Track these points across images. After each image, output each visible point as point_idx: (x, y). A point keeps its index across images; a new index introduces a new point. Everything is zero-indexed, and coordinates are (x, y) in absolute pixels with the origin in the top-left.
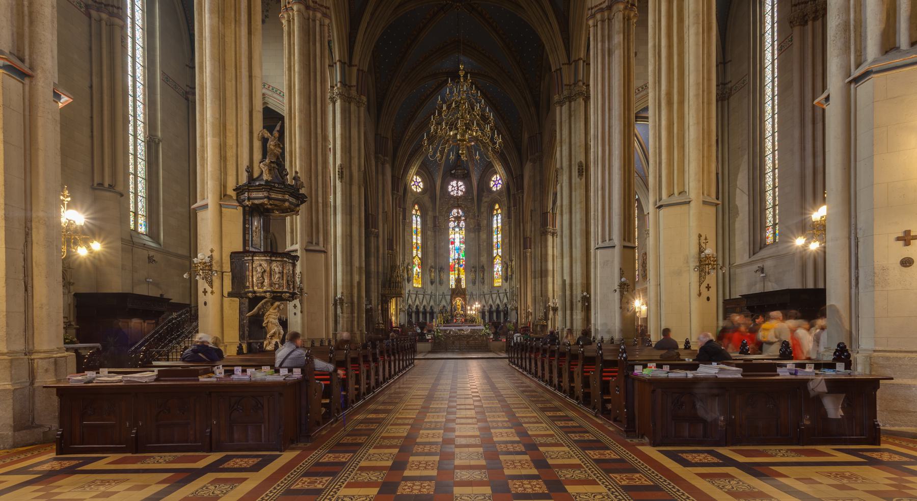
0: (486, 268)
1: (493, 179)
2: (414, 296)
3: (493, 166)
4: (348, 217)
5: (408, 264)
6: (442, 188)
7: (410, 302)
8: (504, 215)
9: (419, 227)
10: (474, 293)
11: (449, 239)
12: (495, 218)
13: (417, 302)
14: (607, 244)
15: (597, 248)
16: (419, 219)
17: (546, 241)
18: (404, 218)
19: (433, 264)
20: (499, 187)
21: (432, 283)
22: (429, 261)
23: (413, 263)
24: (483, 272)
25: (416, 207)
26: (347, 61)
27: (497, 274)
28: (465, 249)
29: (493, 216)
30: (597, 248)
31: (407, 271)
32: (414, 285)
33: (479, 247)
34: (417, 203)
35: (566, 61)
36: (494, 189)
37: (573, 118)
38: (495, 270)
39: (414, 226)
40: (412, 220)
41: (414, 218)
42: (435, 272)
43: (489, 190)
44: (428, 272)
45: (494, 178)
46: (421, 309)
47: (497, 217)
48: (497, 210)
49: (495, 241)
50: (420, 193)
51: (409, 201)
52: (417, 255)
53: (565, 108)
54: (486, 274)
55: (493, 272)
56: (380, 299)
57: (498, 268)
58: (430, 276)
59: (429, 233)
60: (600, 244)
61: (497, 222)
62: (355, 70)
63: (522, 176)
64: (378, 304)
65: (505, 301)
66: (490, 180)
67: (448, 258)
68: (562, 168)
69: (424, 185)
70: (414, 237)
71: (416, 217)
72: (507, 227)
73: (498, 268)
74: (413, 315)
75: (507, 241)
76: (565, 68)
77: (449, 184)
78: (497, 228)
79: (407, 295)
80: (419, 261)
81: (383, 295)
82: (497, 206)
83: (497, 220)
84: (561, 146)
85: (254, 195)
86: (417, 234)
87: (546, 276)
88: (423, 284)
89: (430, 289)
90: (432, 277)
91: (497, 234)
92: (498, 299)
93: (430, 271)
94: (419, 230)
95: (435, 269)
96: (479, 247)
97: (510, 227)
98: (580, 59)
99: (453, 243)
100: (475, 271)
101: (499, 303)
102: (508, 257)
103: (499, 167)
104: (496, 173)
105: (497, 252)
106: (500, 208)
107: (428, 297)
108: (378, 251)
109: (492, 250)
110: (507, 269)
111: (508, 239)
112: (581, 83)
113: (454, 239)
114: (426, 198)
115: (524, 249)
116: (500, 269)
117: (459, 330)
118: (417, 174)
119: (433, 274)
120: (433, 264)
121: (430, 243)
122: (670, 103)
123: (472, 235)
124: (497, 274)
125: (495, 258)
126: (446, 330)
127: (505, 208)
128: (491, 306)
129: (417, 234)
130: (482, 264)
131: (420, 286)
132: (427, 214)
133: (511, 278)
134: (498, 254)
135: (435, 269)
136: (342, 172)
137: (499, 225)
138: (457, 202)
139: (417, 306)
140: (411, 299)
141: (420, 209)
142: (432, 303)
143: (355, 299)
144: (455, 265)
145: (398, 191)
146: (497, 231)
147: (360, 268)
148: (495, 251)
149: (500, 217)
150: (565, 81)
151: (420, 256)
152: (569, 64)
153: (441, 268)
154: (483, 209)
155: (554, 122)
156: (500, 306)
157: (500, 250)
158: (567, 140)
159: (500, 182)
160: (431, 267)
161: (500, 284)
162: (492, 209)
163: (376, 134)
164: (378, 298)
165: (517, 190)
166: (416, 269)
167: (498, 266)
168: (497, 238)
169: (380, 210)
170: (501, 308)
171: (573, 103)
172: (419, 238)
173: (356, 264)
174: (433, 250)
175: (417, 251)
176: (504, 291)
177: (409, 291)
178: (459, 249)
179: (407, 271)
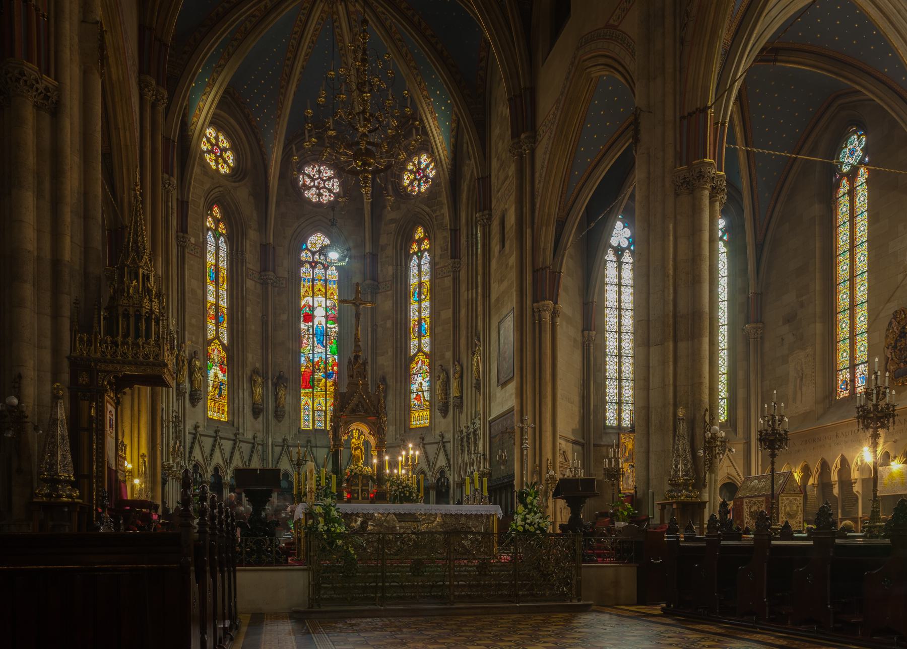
2: (208, 442)
8: (438, 252)
12: (415, 261)
13: (217, 459)
27: (418, 398)
28: (339, 334)
29: (408, 257)
32: (210, 414)
42: (264, 384)
44: (246, 385)
47: (420, 258)
49: (414, 316)
57: (421, 383)
58: (252, 394)
65: (442, 462)
67: (298, 354)
72: (448, 282)
73: (421, 383)
78: (420, 284)
79: (189, 438)
83: (419, 266)
88: (231, 412)
89: (250, 427)
93: (252, 382)
97: (456, 281)
99: (309, 318)
106: (427, 237)
109: (407, 340)
110: (446, 384)
113: (312, 308)
115: (533, 302)
116: (425, 386)
117: (401, 517)
119: (259, 390)
120: (257, 365)
124: (418, 398)
131: (224, 418)
133: (459, 406)
139: (216, 469)
140: (201, 448)
144: (313, 372)
146: (420, 294)
148: (414, 342)
149: (426, 258)
157: (426, 340)
160: (255, 372)
161: (425, 423)
166: (215, 374)
167: (420, 379)
177: (196, 427)
178: (325, 333)
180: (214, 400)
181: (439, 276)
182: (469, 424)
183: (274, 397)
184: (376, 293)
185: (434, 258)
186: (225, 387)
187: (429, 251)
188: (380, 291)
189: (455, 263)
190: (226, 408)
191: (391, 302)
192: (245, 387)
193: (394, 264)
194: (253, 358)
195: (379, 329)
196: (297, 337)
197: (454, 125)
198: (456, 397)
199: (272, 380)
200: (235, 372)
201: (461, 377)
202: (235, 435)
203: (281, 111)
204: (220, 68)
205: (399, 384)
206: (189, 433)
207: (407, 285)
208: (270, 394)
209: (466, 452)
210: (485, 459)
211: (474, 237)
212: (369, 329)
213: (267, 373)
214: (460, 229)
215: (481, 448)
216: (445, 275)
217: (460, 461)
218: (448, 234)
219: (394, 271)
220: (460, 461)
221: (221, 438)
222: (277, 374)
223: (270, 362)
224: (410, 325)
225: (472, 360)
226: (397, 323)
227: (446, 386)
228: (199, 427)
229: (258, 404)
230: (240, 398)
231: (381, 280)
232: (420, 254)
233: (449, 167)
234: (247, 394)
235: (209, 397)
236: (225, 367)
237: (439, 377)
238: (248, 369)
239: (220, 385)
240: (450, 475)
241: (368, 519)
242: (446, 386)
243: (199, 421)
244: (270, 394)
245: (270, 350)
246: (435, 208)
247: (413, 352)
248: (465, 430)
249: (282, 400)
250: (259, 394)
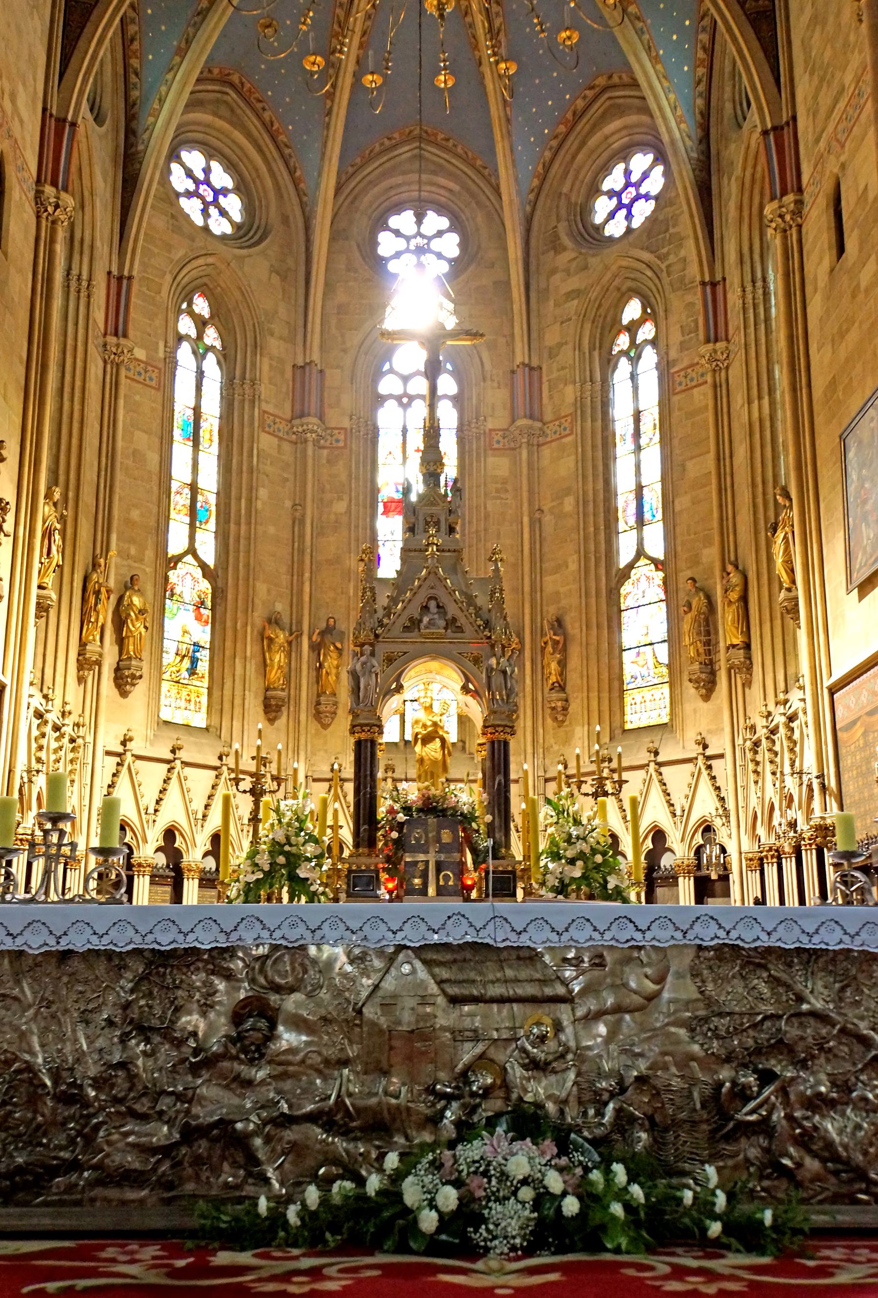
0: (573, 627)
1: (606, 185)
8: (676, 337)
9: (212, 406)
11: (375, 491)
12: (624, 365)
16: (211, 364)
22: (262, 588)
23: (165, 589)
24: (562, 649)
25: (201, 306)
29: (609, 363)
31: (120, 622)
32: (166, 714)
33: (536, 523)
36: (616, 229)
38: (629, 636)
40: (171, 363)
41: (185, 354)
47: (635, 361)
48: (633, 328)
50: (224, 237)
52: (192, 550)
54: (574, 662)
55: (616, 650)
59: (266, 442)
66: (595, 191)
69: (249, 208)
71: (200, 357)
78: (637, 416)
80: (205, 586)
82: (633, 310)
83: (633, 377)
91: (638, 448)
93: (265, 642)
96: (536, 523)
101: (666, 823)
102: (711, 554)
111: (712, 455)
119: (279, 658)
120: (279, 607)
125: (625, 574)
130: (551, 611)
134: (640, 553)
135: (295, 634)
139: (170, 834)
146: (637, 434)
149: (650, 356)
151: (210, 561)
154: (552, 337)
156: (674, 839)
160: (273, 621)
162: (614, 326)
174: (286, 535)
176: (694, 751)
180: (178, 682)
181: (679, 389)
182: (771, 707)
183: (314, 674)
184: (539, 445)
185: (667, 354)
186: (204, 656)
187: (654, 342)
188: (549, 439)
189: (715, 351)
190: (204, 699)
191: (573, 457)
192: (248, 653)
193: (578, 379)
194: (269, 591)
195: (548, 519)
197: (701, 71)
198: (734, 646)
199: (310, 638)
200: (229, 624)
201: (744, 598)
202: (220, 758)
203: (333, 101)
204: (200, 17)
205: (594, 631)
206: (108, 753)
207: (606, 421)
208: (305, 667)
209: (769, 777)
210: (824, 788)
211: (759, 284)
212: (526, 520)
213: (300, 622)
214: (724, 279)
215: (810, 762)
216: (694, 383)
217: (754, 802)
218: (696, 297)
219: (579, 394)
220: (754, 802)
221: (186, 764)
222: (323, 625)
223: (306, 598)
224: (616, 503)
225: (769, 545)
226: (585, 503)
227: (708, 625)
228: (131, 740)
229: (275, 689)
230: (237, 678)
231: (548, 416)
232: (634, 354)
233: (694, 155)
234: (252, 668)
235: (166, 676)
236: (206, 613)
237: (689, 605)
238: (256, 614)
239: (194, 652)
240: (730, 836)
241: (277, 989)
242: (708, 625)
243: (133, 727)
244: (305, 667)
245: (307, 575)
246: (665, 250)
248: (760, 722)
249: (332, 678)
250: (280, 667)
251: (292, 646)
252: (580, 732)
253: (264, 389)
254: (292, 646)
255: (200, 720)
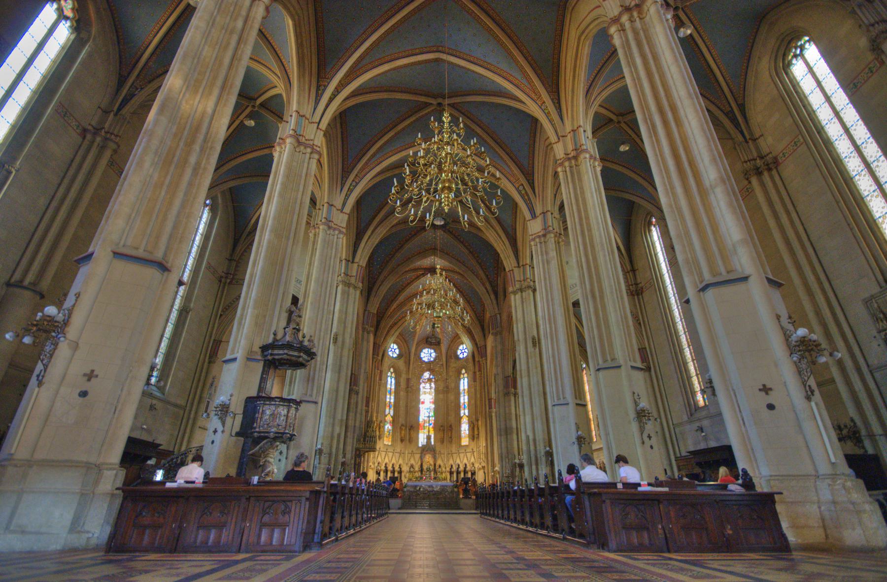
0: (454, 427)
3: (460, 338)
4: (337, 375)
5: (381, 422)
6: (415, 354)
7: (379, 459)
9: (393, 387)
10: (442, 452)
12: (462, 381)
13: (387, 460)
14: (562, 402)
15: (554, 405)
17: (510, 401)
18: (380, 379)
19: (404, 422)
20: (465, 354)
21: (402, 441)
22: (400, 419)
25: (392, 370)
26: (351, 259)
29: (460, 380)
30: (554, 405)
31: (379, 428)
33: (447, 407)
34: (393, 367)
35: (516, 265)
36: (461, 356)
37: (525, 304)
38: (462, 429)
39: (389, 386)
41: (389, 379)
43: (457, 357)
44: (399, 430)
45: (461, 347)
46: (390, 468)
48: (463, 374)
49: (462, 401)
51: (386, 362)
53: (518, 296)
55: (460, 431)
56: (354, 453)
57: (465, 427)
60: (556, 402)
61: (464, 384)
62: (355, 265)
63: (485, 346)
64: (352, 458)
66: (457, 349)
68: (519, 340)
69: (400, 351)
70: (388, 396)
72: (473, 390)
73: (465, 427)
74: (382, 473)
75: (473, 402)
76: (516, 270)
77: (421, 351)
81: (357, 449)
82: (463, 371)
84: (517, 324)
85: (276, 352)
86: (390, 394)
87: (511, 433)
89: (399, 447)
90: (403, 435)
92: (465, 459)
93: (401, 429)
94: (393, 390)
95: (406, 427)
97: (475, 390)
98: (526, 264)
100: (444, 430)
102: (474, 417)
103: (465, 339)
104: (462, 343)
105: (464, 412)
107: (397, 455)
108: (357, 407)
112: (529, 280)
114: (401, 364)
118: (394, 343)
119: (403, 432)
120: (404, 422)
121: (402, 403)
122: (594, 296)
123: (441, 396)
126: (416, 486)
127: (471, 373)
128: (459, 465)
129: (390, 394)
132: (400, 376)
133: (478, 438)
135: (406, 427)
136: (336, 338)
137: (466, 387)
138: (430, 366)
141: (395, 371)
142: (401, 462)
143: (334, 450)
145: (378, 355)
147: (342, 420)
148: (462, 412)
149: (466, 380)
150: (517, 278)
152: (519, 267)
153: (412, 427)
154: (451, 374)
155: (510, 307)
157: (467, 412)
158: (522, 319)
159: (466, 350)
160: (402, 425)
161: (467, 443)
162: (459, 373)
163: (365, 310)
164: (352, 451)
165: (482, 358)
166: (388, 427)
168: (464, 399)
169: (362, 371)
170: (468, 468)
171: (524, 293)
172: (392, 397)
173: (339, 416)
175: (390, 409)
179: (379, 428)
196: (418, 411)
247: (462, 415)
251: (406, 429)
252: (454, 445)
253: (402, 384)
254: (406, 429)
255: (390, 444)
